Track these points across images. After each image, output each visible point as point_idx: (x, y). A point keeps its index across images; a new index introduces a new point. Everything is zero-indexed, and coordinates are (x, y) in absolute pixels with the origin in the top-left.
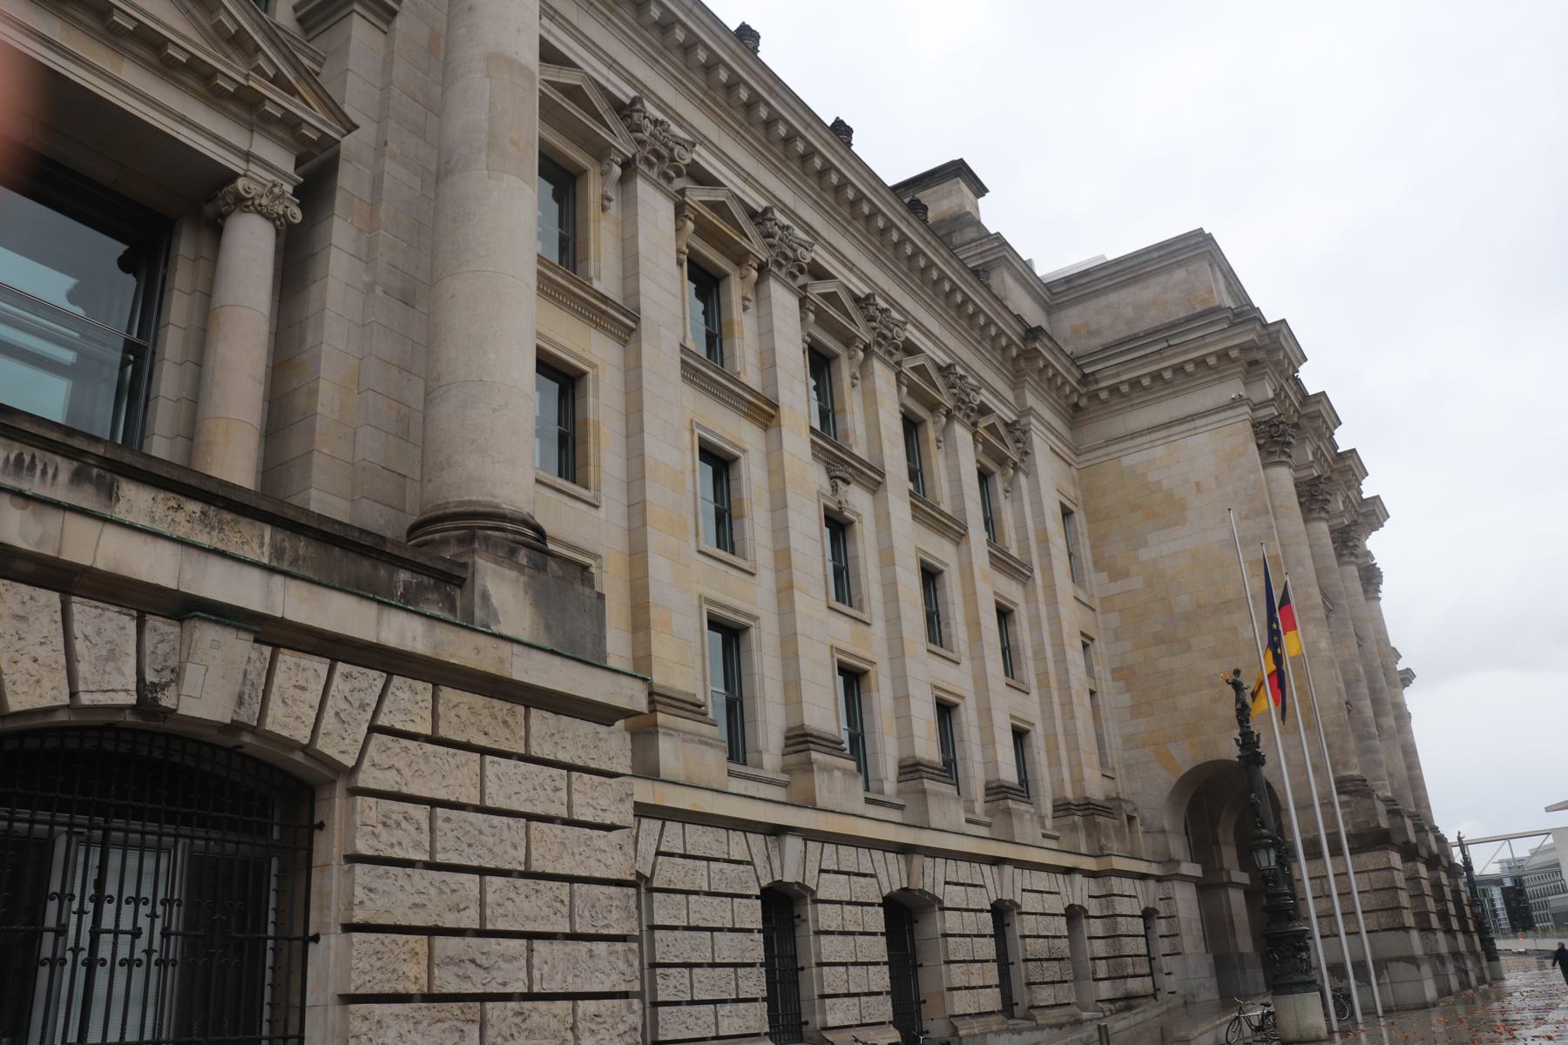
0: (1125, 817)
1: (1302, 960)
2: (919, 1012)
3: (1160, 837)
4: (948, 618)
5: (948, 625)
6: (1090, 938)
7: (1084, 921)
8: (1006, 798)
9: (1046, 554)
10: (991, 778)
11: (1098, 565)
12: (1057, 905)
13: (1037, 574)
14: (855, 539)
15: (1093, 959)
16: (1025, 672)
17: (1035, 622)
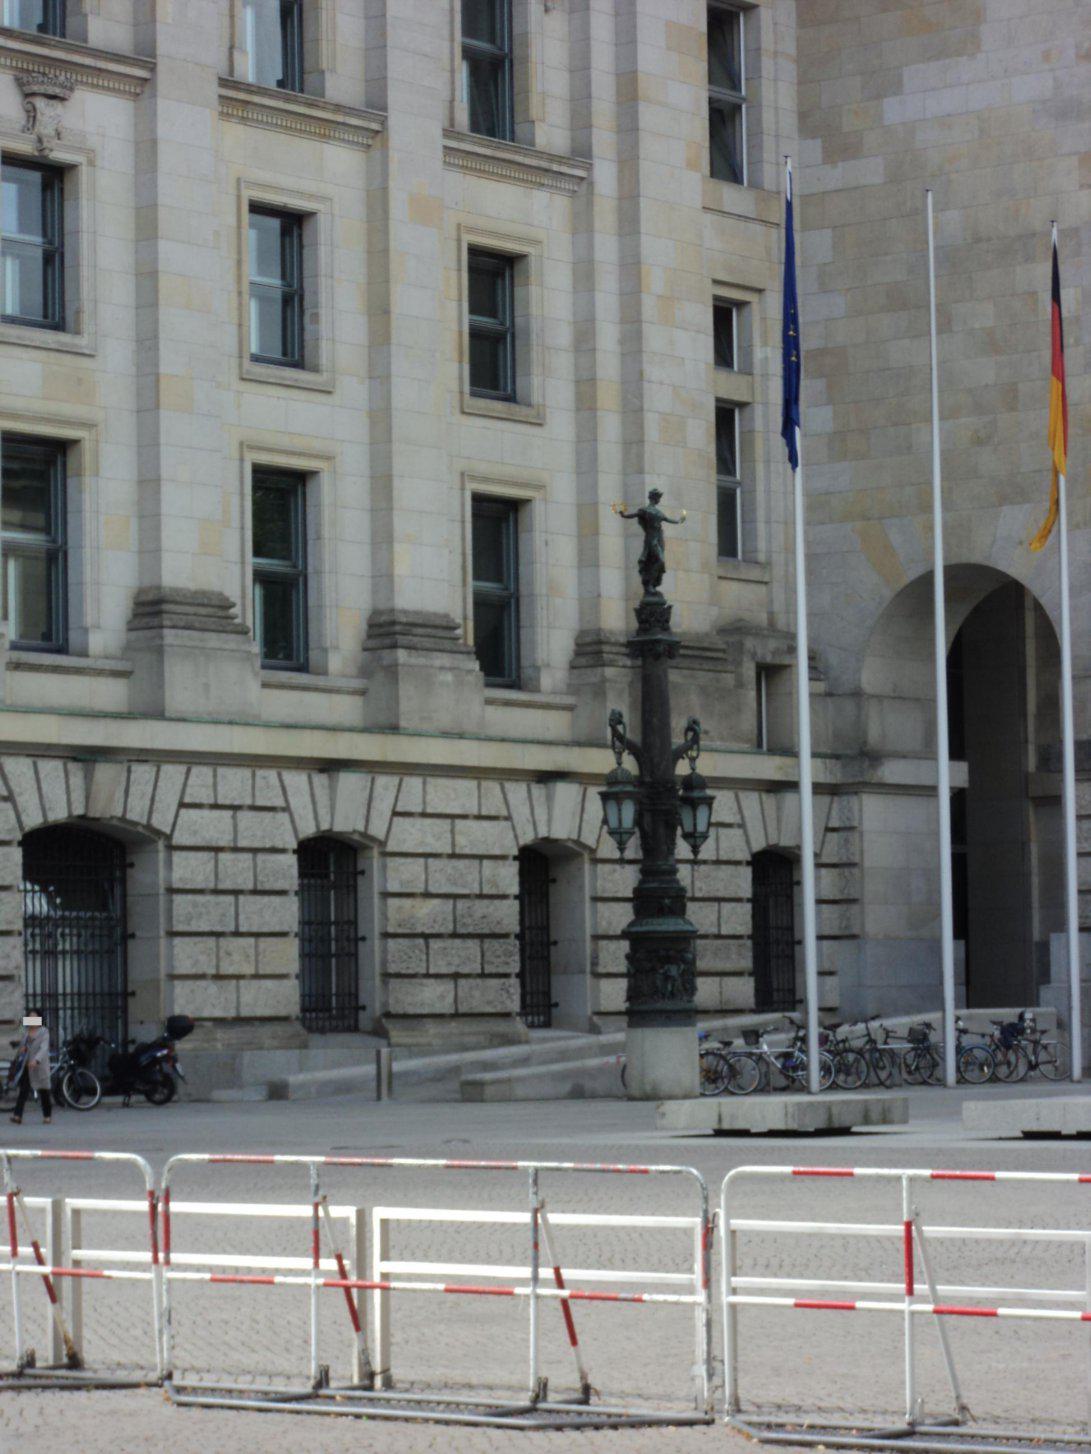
0: (749, 671)
1: (667, 977)
2: (125, 1010)
3: (849, 706)
4: (316, 305)
5: (316, 317)
6: (596, 899)
7: (587, 866)
8: (394, 646)
9: (628, 127)
10: (382, 606)
11: (810, 121)
12: (503, 840)
13: (605, 175)
14: (77, 199)
15: (596, 938)
16: (536, 381)
17: (584, 275)
